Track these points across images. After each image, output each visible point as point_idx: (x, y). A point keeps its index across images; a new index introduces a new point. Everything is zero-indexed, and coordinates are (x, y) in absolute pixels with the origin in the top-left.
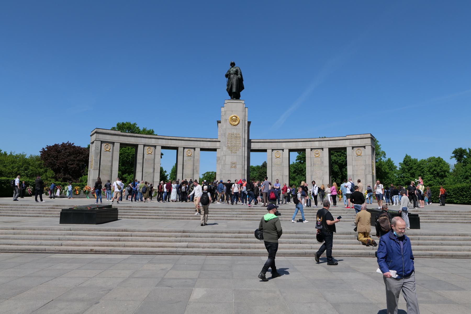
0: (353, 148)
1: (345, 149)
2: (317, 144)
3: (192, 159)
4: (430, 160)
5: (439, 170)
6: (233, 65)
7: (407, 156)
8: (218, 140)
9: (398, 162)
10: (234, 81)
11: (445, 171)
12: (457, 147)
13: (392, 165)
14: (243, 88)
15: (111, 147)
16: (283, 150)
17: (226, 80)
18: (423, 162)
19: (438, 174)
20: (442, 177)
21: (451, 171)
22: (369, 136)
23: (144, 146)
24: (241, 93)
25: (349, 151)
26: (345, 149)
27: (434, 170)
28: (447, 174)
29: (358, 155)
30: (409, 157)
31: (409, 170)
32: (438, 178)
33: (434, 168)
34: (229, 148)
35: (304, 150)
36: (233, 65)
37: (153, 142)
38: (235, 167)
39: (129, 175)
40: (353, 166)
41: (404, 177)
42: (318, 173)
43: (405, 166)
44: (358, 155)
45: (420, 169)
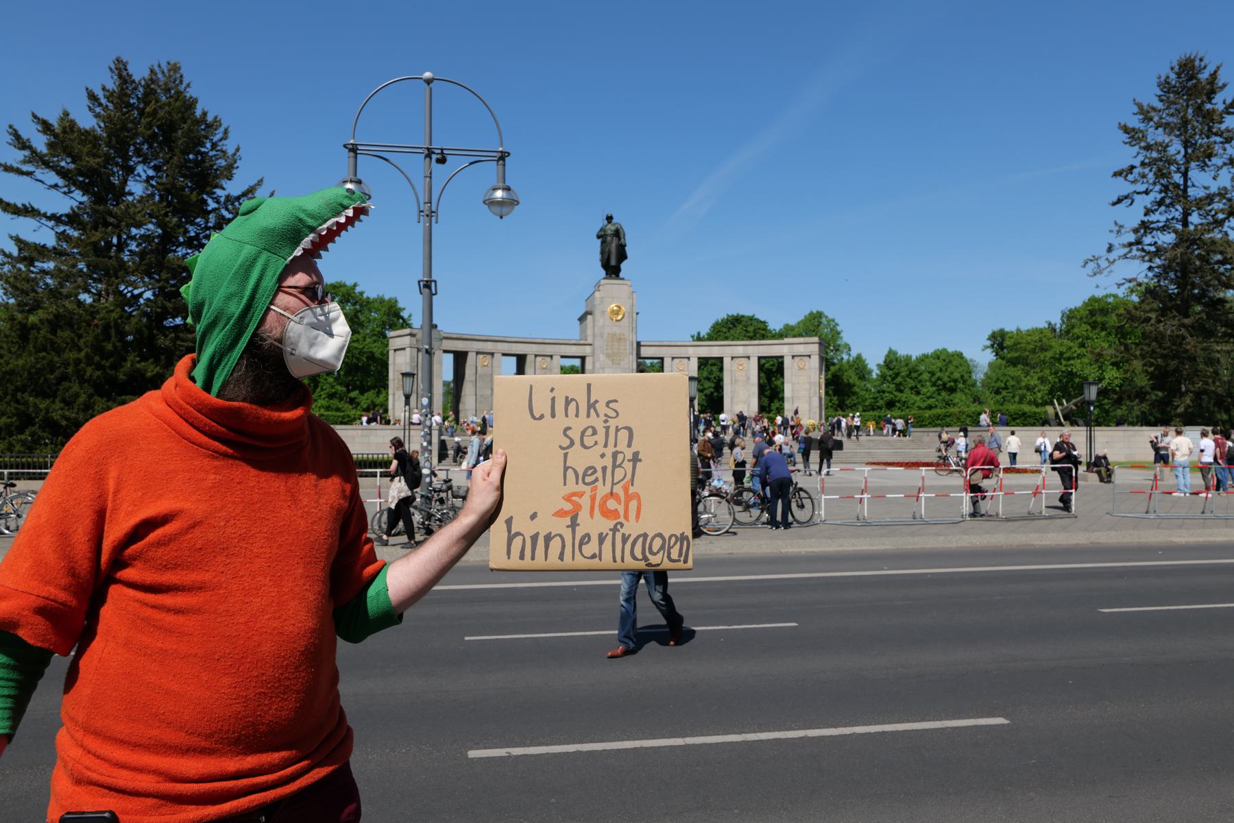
0: (793, 357)
4: (937, 355)
5: (946, 379)
6: (609, 219)
7: (890, 351)
8: (589, 341)
9: (874, 361)
10: (613, 247)
11: (956, 381)
12: (996, 328)
13: (865, 366)
14: (625, 257)
17: (599, 241)
18: (923, 359)
19: (944, 384)
20: (952, 390)
21: (979, 376)
23: (478, 353)
24: (623, 266)
27: (939, 379)
28: (961, 386)
29: (801, 369)
30: (895, 353)
31: (893, 379)
32: (943, 393)
33: (939, 374)
34: (608, 356)
36: (609, 219)
39: (362, 393)
40: (793, 385)
41: (884, 392)
42: (741, 396)
43: (885, 370)
44: (801, 369)
45: (914, 375)
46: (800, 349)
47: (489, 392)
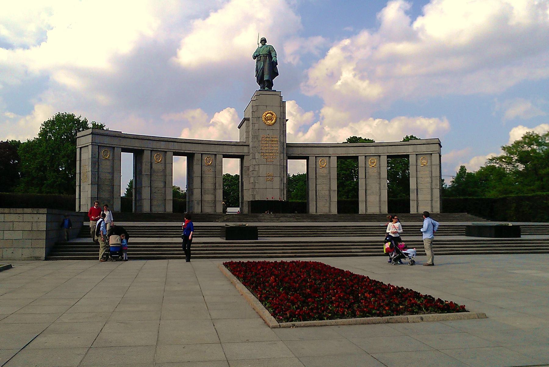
0: (417, 155)
1: (407, 156)
2: (372, 150)
3: (212, 170)
6: (264, 41)
8: (246, 144)
15: (111, 155)
16: (330, 157)
22: (437, 141)
23: (151, 151)
25: (412, 160)
26: (407, 156)
35: (357, 158)
36: (264, 41)
37: (162, 146)
38: (271, 180)
46: (423, 149)
47: (161, 185)
